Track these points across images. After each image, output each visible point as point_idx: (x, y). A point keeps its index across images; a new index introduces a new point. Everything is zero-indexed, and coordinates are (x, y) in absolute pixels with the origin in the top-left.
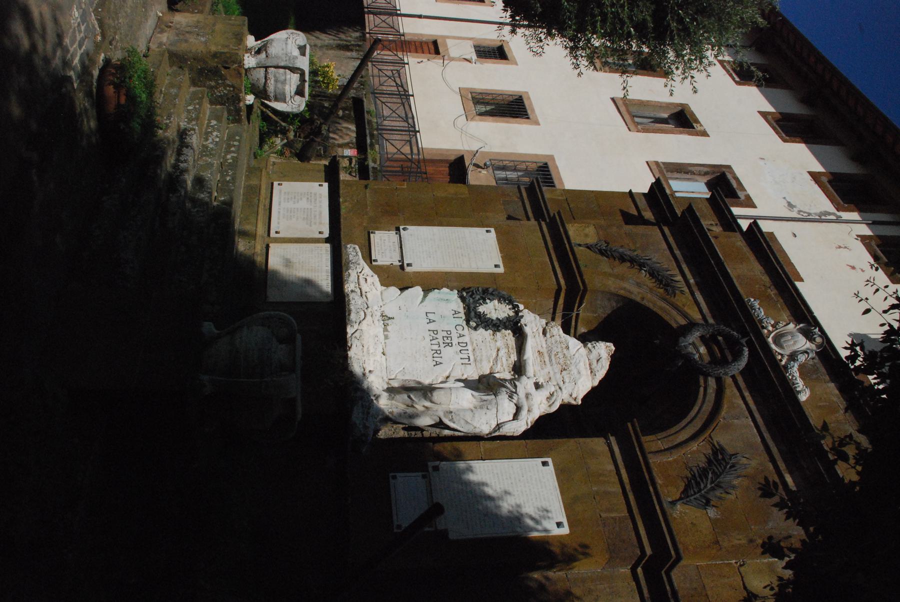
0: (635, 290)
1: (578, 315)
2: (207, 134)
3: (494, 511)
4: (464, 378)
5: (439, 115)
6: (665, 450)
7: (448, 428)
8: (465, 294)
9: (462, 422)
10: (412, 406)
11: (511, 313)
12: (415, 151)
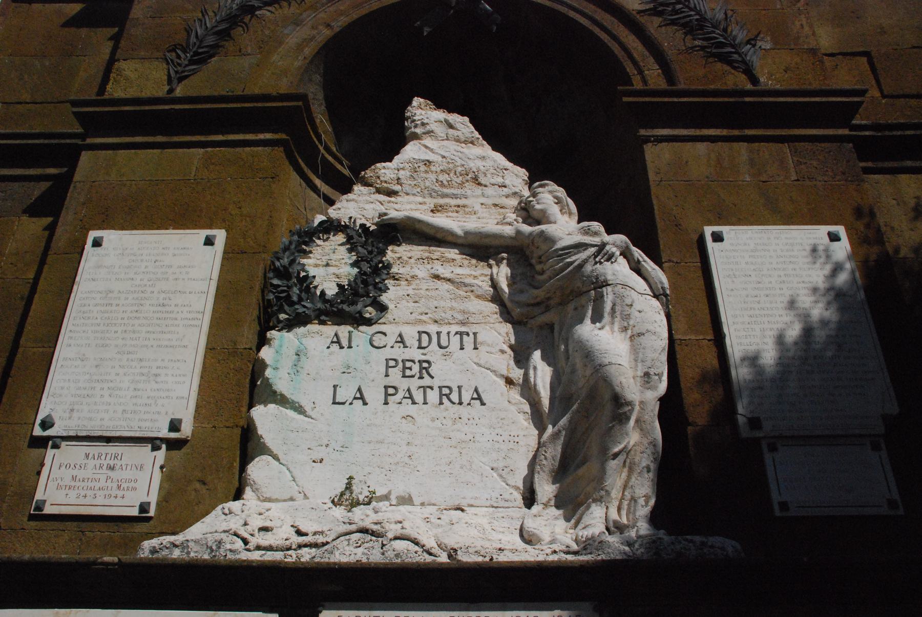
0: (303, 32)
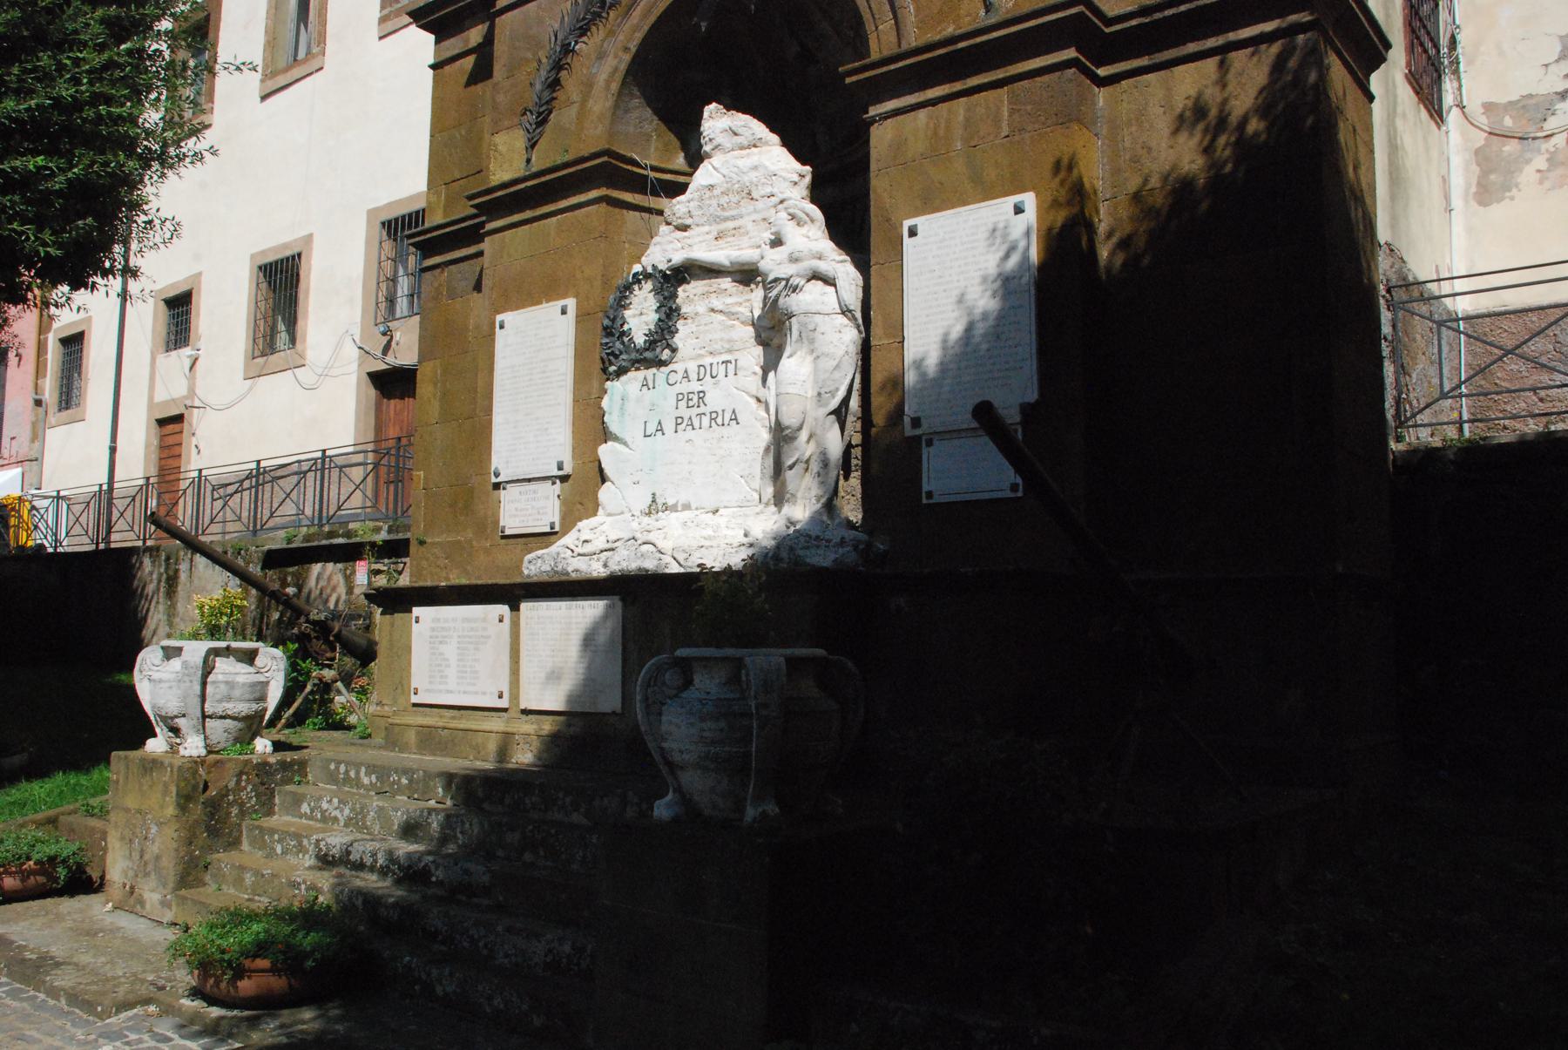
0: (610, 62)
1: (654, 169)
2: (326, 818)
3: (991, 322)
4: (760, 372)
5: (296, 416)
6: (895, 17)
7: (846, 401)
8: (612, 369)
9: (837, 375)
10: (807, 462)
11: (648, 286)
12: (359, 458)
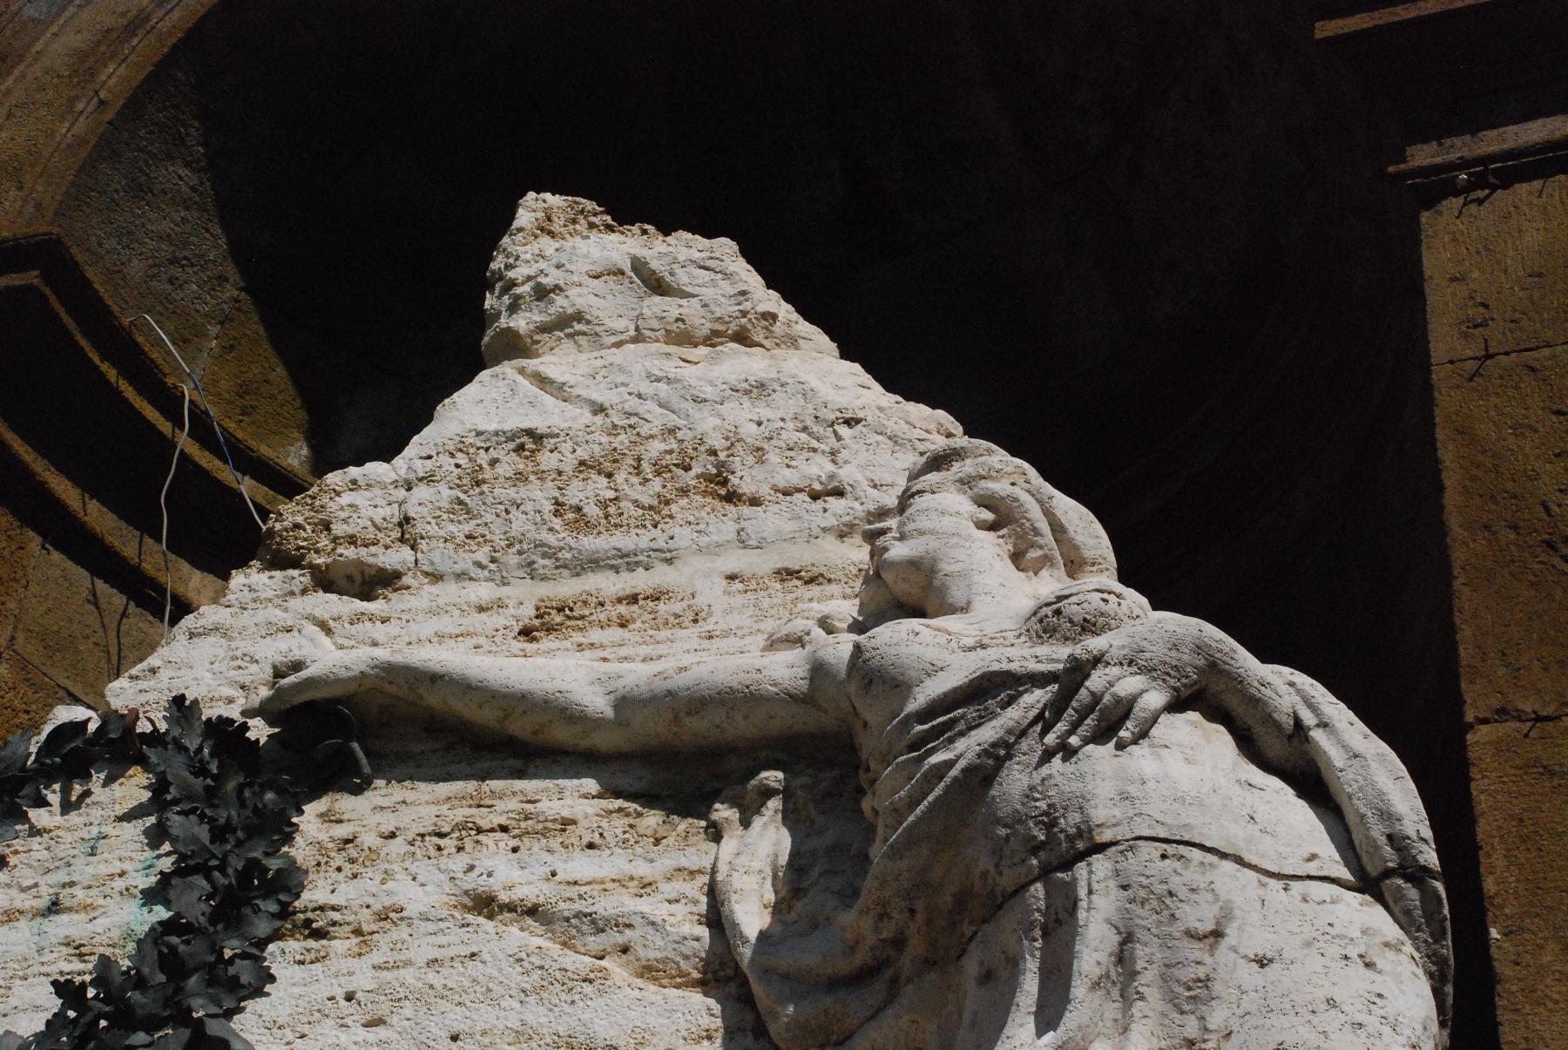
11: (134, 788)
